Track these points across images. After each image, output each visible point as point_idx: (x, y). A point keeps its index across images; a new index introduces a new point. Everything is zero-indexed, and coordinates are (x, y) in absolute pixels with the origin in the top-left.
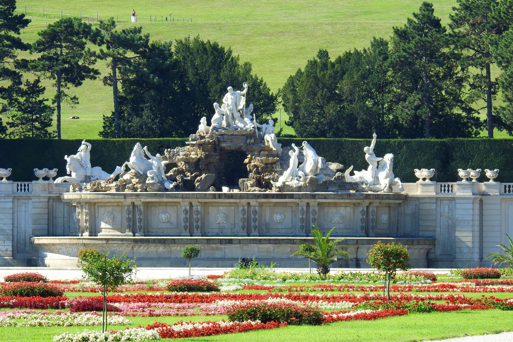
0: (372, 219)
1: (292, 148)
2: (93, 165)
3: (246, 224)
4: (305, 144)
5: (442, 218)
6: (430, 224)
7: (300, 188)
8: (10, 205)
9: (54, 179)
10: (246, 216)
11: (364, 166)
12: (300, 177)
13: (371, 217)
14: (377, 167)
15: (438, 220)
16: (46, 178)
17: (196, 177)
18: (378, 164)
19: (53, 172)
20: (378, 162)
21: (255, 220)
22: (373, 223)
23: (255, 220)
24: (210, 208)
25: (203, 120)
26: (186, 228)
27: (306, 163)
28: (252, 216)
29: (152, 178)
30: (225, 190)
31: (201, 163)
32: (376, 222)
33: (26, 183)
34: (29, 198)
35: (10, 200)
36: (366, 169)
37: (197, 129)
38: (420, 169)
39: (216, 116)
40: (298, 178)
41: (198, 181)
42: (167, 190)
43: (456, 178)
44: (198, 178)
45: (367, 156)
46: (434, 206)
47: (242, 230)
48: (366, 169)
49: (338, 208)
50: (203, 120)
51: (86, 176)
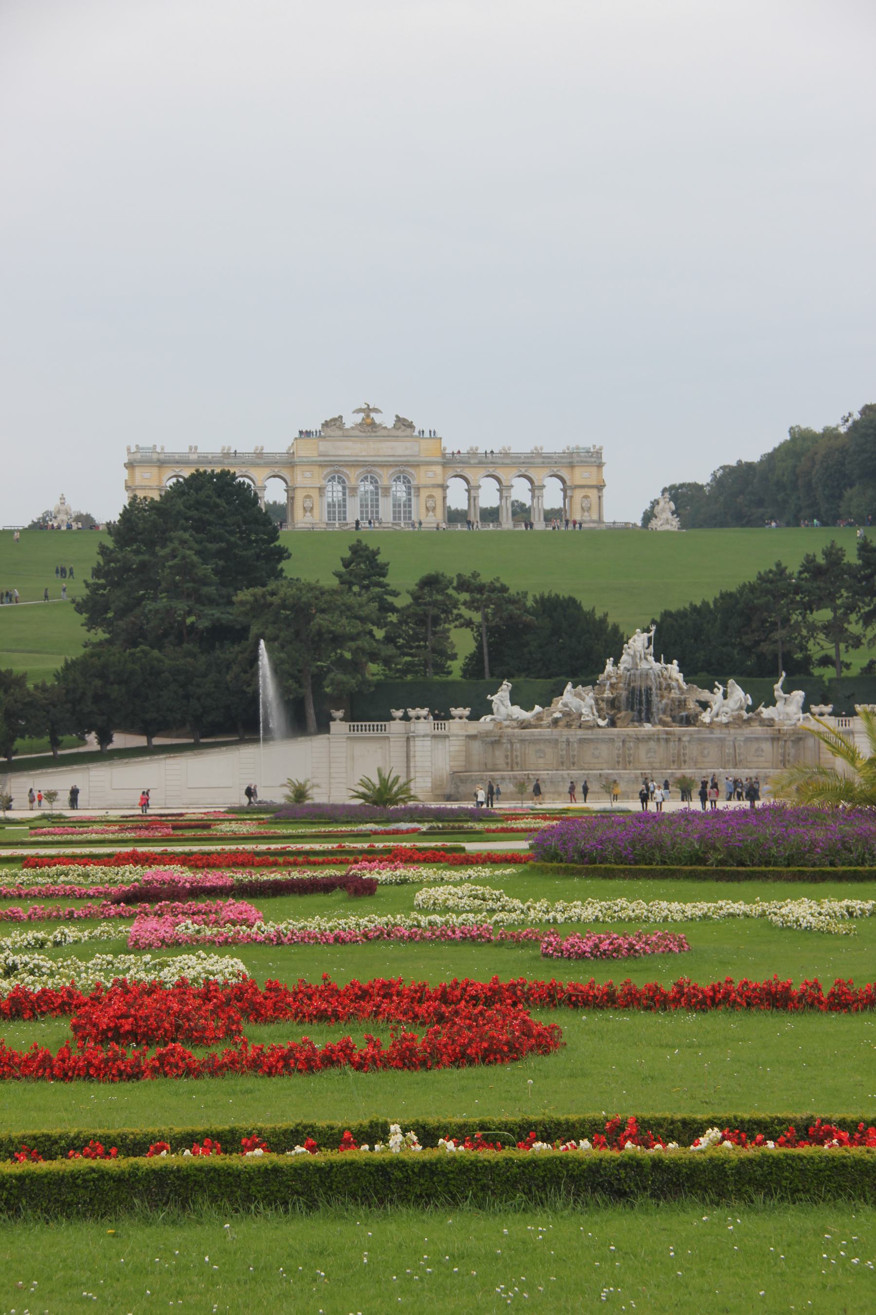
1: (716, 687)
2: (513, 704)
4: (731, 681)
7: (727, 725)
8: (429, 743)
9: (474, 717)
11: (771, 702)
16: (461, 718)
17: (615, 715)
19: (467, 712)
21: (684, 755)
23: (684, 755)
25: (610, 661)
27: (729, 700)
28: (682, 751)
29: (588, 716)
30: (648, 727)
33: (443, 722)
34: (446, 737)
36: (774, 705)
37: (605, 668)
39: (624, 658)
41: (619, 719)
42: (599, 726)
43: (853, 713)
44: (619, 716)
45: (776, 693)
48: (774, 705)
50: (610, 661)
51: (508, 715)
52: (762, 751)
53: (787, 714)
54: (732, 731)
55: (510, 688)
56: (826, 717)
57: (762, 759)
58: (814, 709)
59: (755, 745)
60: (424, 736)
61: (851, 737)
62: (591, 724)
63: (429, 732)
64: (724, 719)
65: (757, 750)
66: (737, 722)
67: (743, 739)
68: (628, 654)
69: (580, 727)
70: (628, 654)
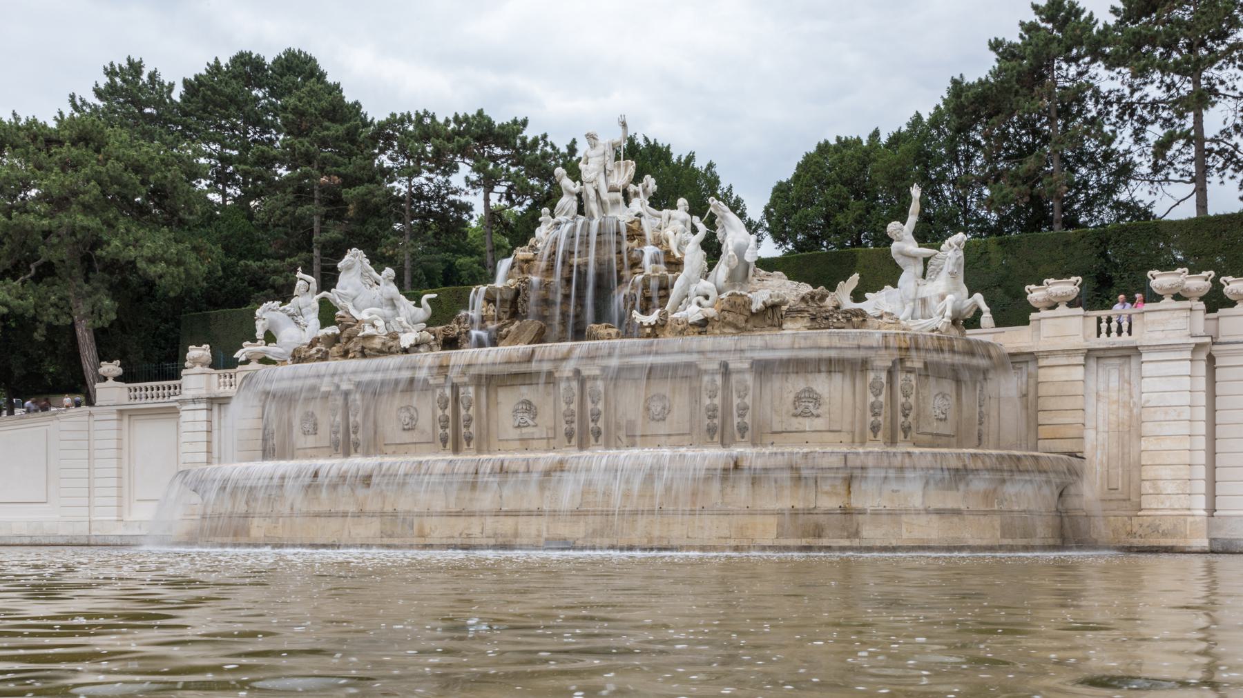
0: (903, 405)
3: (575, 426)
5: (1100, 405)
6: (1067, 418)
7: (703, 325)
10: (574, 407)
12: (707, 297)
13: (901, 399)
14: (924, 276)
15: (1090, 410)
18: (925, 269)
20: (926, 261)
21: (596, 416)
22: (906, 416)
23: (596, 416)
24: (500, 390)
26: (444, 441)
31: (519, 299)
32: (918, 415)
35: (203, 406)
36: (895, 286)
38: (1039, 283)
40: (701, 299)
42: (406, 351)
45: (894, 247)
46: (1078, 373)
47: (566, 440)
49: (810, 377)
52: (817, 400)
53: (924, 301)
54: (707, 342)
55: (314, 286)
56: (1063, 310)
57: (819, 423)
58: (1035, 294)
59: (796, 384)
60: (194, 401)
61: (1134, 361)
62: (377, 343)
63: (203, 393)
64: (693, 313)
65: (798, 398)
66: (730, 317)
67: (746, 366)
68: (571, 193)
69: (364, 355)
70: (571, 193)
